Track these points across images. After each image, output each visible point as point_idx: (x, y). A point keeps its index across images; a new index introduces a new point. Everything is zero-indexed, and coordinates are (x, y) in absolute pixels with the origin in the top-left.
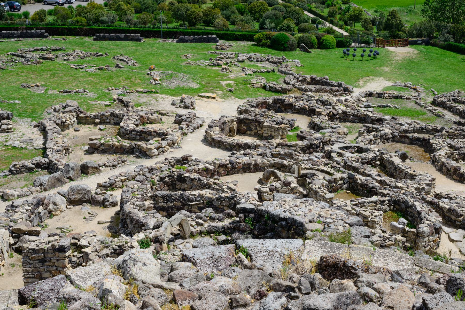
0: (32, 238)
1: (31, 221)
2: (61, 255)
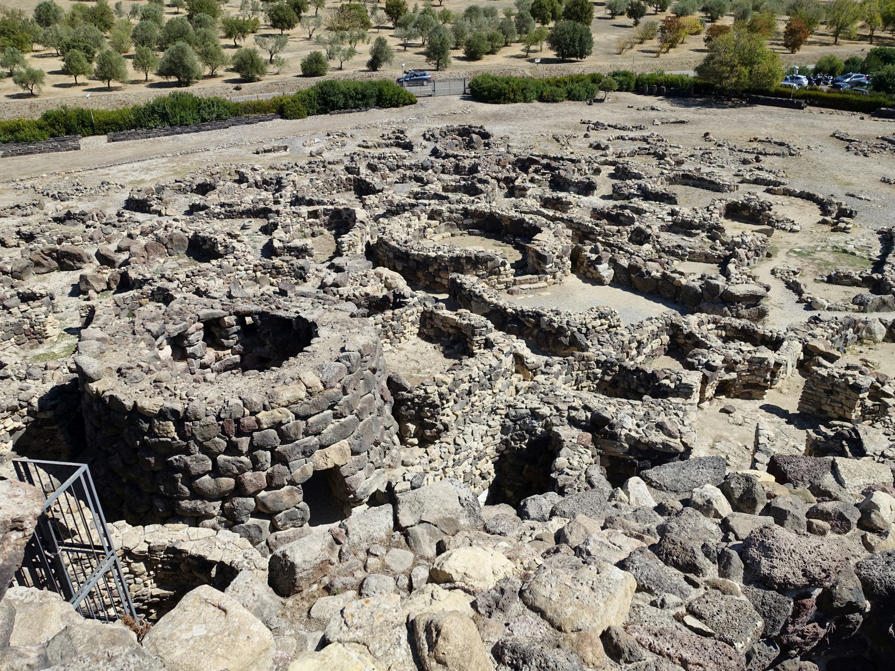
0: (825, 362)
1: (832, 342)
2: (853, 394)
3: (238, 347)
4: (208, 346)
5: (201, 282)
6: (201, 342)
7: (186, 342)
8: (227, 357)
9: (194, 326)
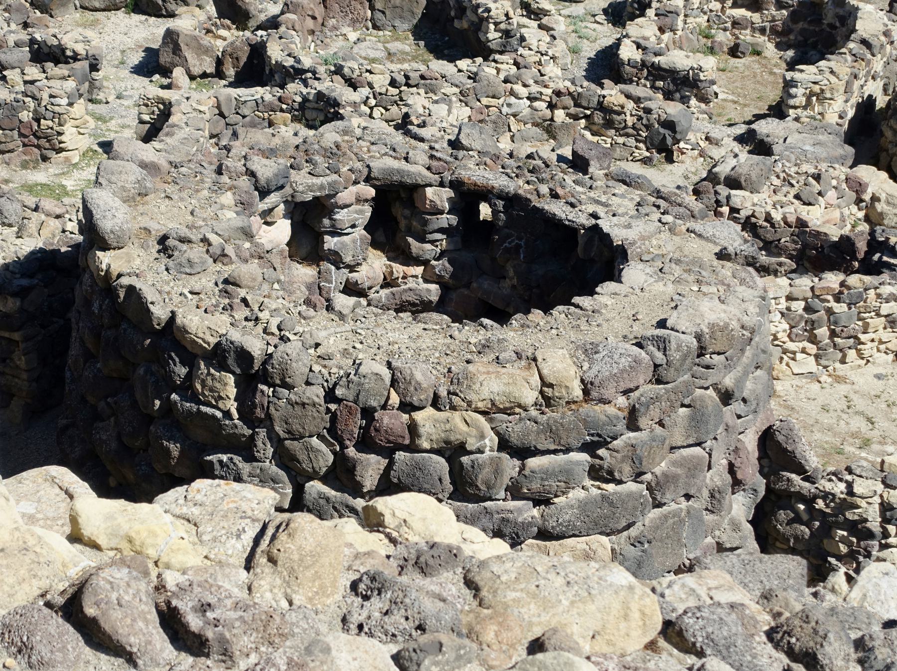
3: (442, 266)
4: (375, 245)
5: (417, 101)
6: (360, 232)
7: (326, 222)
8: (411, 283)
9: (353, 189)
